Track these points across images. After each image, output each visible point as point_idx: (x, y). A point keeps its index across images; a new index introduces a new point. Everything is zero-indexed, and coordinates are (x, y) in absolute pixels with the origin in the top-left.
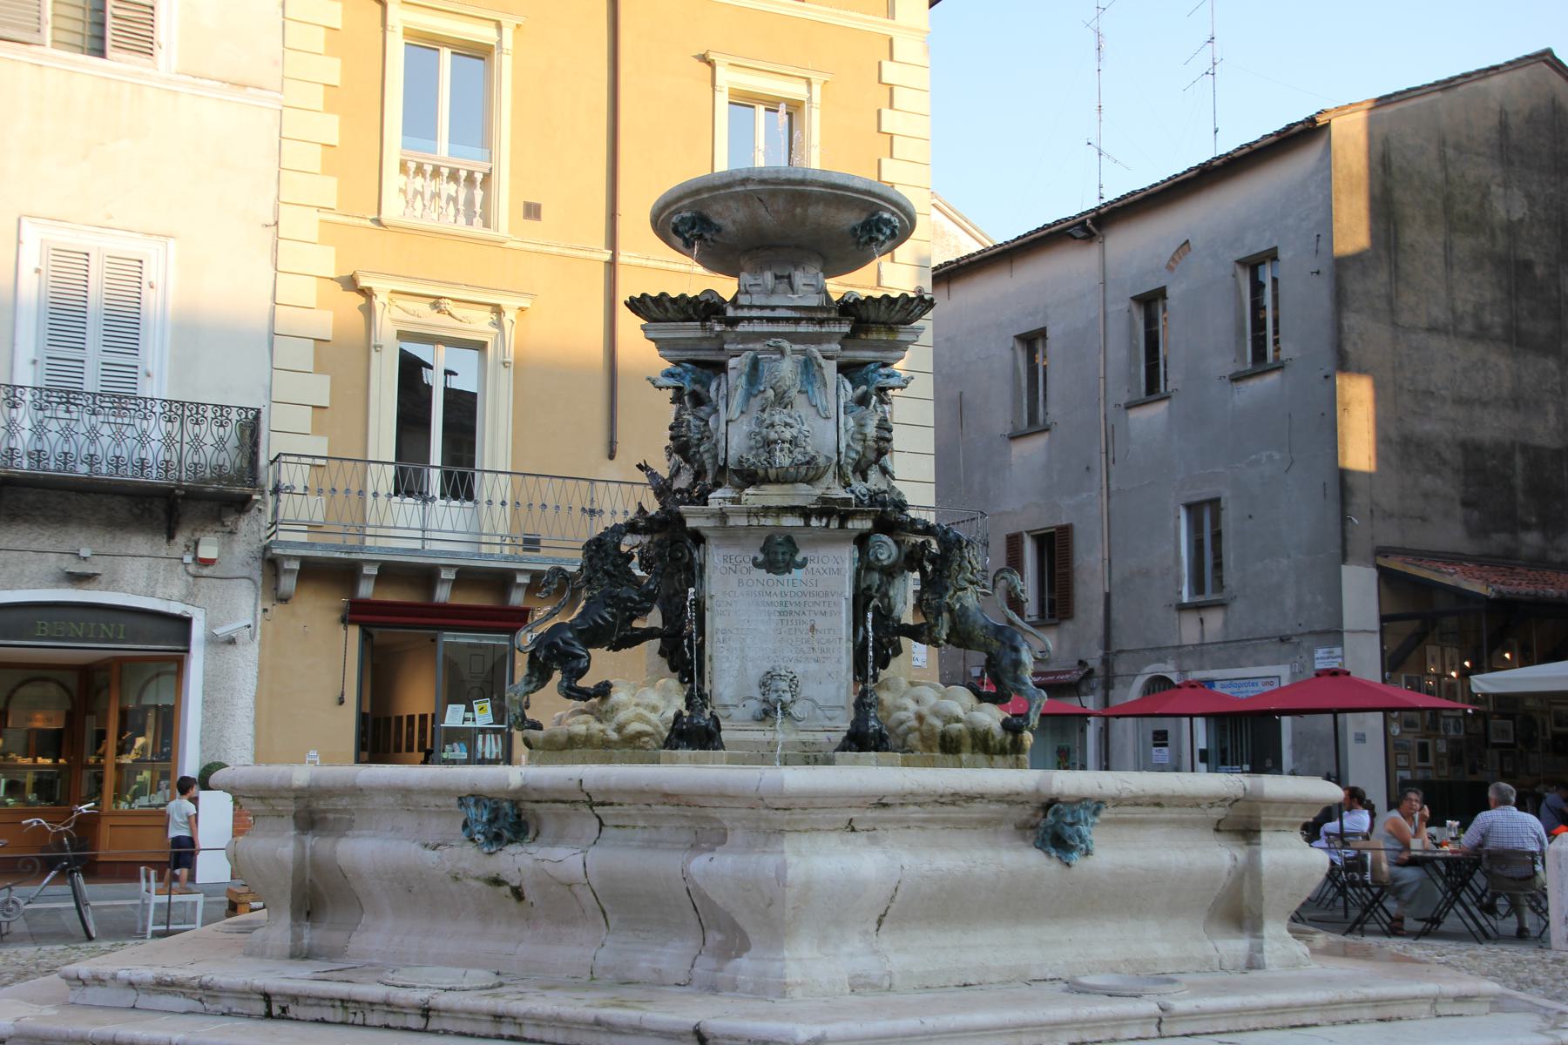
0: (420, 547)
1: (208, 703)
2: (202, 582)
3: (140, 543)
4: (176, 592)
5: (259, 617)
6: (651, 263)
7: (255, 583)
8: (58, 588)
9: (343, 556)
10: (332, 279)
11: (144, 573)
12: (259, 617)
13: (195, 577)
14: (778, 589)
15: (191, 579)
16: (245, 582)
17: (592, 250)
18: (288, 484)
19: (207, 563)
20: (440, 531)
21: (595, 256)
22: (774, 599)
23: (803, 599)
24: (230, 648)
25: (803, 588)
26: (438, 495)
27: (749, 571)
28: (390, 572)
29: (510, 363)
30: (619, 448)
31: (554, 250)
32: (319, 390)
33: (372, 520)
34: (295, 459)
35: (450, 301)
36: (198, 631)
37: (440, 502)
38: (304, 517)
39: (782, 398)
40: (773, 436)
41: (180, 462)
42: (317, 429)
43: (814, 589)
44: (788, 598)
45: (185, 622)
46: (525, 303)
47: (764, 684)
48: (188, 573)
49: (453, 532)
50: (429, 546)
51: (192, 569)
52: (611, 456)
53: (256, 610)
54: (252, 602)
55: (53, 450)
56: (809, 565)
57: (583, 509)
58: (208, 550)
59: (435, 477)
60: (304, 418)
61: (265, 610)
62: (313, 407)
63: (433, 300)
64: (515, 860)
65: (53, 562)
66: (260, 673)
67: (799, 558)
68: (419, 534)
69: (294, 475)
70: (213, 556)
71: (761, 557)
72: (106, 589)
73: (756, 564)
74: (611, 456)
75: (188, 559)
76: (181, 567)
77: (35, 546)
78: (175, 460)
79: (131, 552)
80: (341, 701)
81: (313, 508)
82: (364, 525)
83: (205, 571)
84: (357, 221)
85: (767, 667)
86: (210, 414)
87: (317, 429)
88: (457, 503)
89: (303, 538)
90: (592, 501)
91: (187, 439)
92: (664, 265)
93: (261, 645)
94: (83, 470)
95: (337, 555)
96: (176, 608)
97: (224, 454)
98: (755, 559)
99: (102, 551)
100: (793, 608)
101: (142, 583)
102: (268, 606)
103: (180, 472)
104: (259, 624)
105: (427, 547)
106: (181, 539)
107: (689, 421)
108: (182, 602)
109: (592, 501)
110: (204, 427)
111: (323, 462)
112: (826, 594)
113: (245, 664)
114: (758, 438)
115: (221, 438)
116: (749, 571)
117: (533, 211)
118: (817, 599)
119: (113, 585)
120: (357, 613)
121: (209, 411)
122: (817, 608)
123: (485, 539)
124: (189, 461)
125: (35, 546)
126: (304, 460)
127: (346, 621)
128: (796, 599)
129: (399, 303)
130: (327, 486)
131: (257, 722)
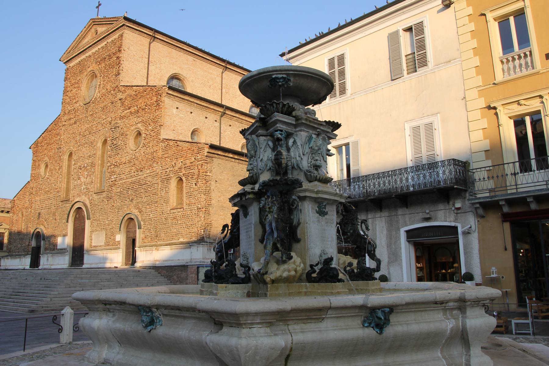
0: (494, 195)
1: (465, 253)
2: (459, 215)
3: (441, 206)
5: (476, 224)
7: (473, 212)
8: (423, 222)
9: (490, 200)
10: (484, 108)
11: (443, 215)
13: (457, 213)
15: (455, 215)
16: (471, 213)
19: (458, 209)
24: (469, 235)
26: (536, 169)
28: (511, 202)
33: (508, 184)
34: (479, 170)
35: (523, 101)
36: (460, 230)
37: (536, 172)
38: (485, 188)
41: (434, 181)
42: (487, 158)
45: (456, 228)
48: (455, 213)
49: (533, 183)
51: (455, 211)
53: (475, 221)
54: (473, 219)
58: (458, 205)
59: (533, 163)
61: (478, 221)
62: (485, 151)
63: (517, 102)
65: (421, 216)
66: (479, 241)
72: (435, 221)
75: (453, 209)
76: (452, 212)
77: (417, 212)
78: (433, 180)
79: (439, 209)
80: (506, 249)
81: (490, 184)
82: (506, 186)
83: (459, 211)
84: (488, 86)
87: (487, 158)
88: (527, 173)
89: (488, 195)
93: (478, 233)
94: (412, 189)
95: (488, 200)
96: (453, 224)
97: (445, 176)
99: (432, 210)
101: (443, 218)
102: (479, 219)
104: (477, 226)
105: (518, 191)
106: (451, 203)
108: (454, 222)
110: (445, 167)
111: (491, 168)
113: (474, 238)
115: (444, 171)
119: (436, 220)
120: (506, 218)
121: (440, 163)
125: (417, 212)
126: (482, 169)
127: (504, 221)
129: (507, 107)
130: (495, 176)
131: (480, 258)
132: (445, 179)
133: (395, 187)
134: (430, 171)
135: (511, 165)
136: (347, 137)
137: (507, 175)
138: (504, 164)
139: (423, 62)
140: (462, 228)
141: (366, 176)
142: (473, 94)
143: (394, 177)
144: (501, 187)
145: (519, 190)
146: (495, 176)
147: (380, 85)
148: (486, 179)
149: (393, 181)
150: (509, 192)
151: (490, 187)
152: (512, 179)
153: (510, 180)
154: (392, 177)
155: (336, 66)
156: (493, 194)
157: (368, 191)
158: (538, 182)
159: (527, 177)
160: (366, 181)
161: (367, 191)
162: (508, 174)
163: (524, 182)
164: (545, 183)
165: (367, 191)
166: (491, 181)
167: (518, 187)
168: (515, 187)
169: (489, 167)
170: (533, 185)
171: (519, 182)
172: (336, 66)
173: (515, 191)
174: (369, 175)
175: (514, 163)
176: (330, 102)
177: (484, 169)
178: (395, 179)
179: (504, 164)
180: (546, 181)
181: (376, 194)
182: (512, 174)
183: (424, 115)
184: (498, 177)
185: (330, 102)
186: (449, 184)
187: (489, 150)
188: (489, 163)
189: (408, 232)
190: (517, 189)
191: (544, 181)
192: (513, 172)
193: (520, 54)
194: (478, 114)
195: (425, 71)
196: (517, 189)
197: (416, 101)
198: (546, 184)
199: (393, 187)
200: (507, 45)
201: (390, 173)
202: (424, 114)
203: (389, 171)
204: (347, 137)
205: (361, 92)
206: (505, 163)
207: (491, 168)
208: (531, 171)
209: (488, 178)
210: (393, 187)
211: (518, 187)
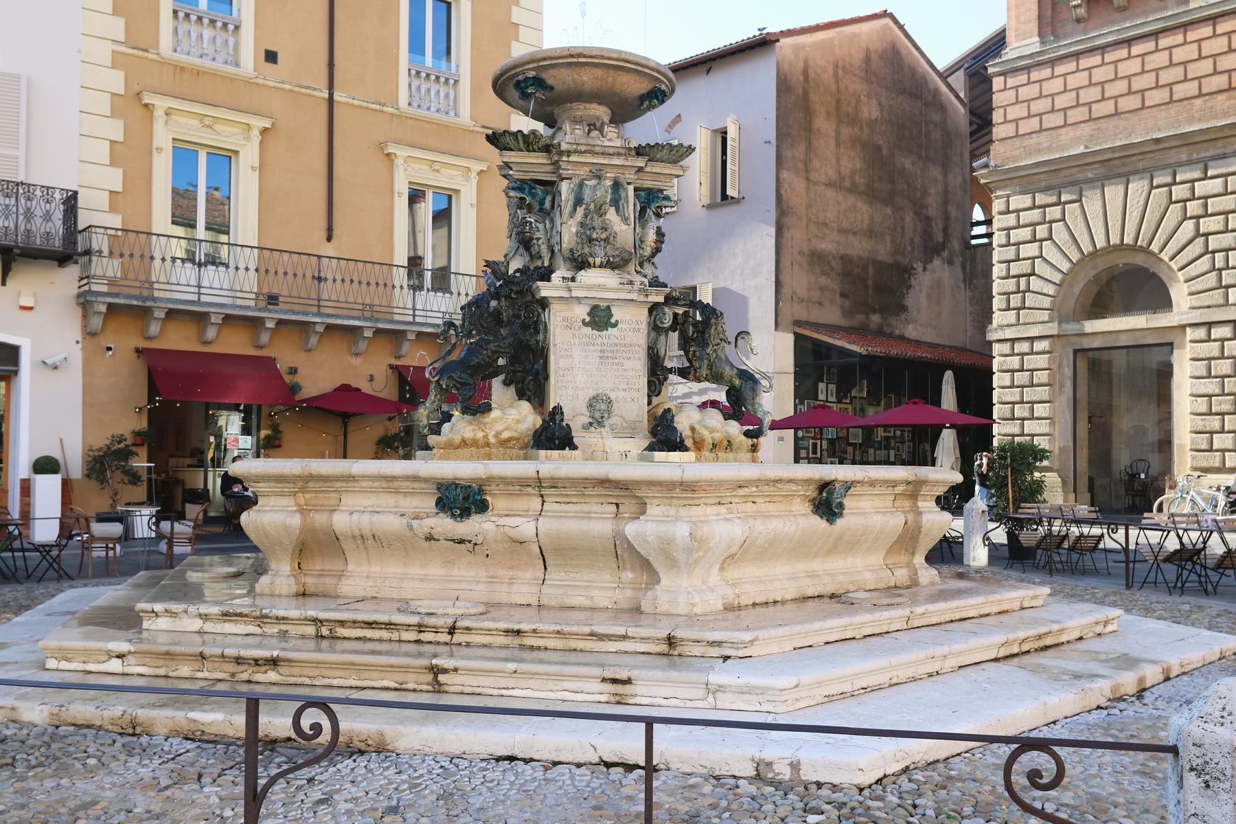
6: (355, 102)
9: (140, 304)
14: (599, 341)
17: (315, 89)
18: (97, 249)
20: (241, 291)
21: (316, 93)
22: (596, 348)
23: (616, 348)
25: (616, 341)
27: (580, 328)
30: (336, 232)
31: (288, 87)
32: (114, 179)
39: (600, 209)
40: (594, 236)
42: (113, 208)
43: (623, 342)
44: (606, 348)
46: (267, 124)
47: (591, 405)
50: (203, 298)
52: (329, 239)
56: (620, 326)
57: (313, 277)
62: (110, 191)
64: (474, 526)
67: (613, 321)
68: (196, 290)
69: (100, 242)
71: (588, 319)
73: (585, 324)
74: (329, 239)
78: (12, 226)
85: (592, 393)
86: (38, 193)
87: (113, 208)
90: (319, 271)
91: (21, 211)
92: (365, 104)
97: (50, 224)
98: (584, 320)
100: (609, 354)
103: (17, 236)
107: (531, 222)
109: (319, 271)
110: (34, 202)
111: (120, 233)
112: (630, 345)
114: (583, 237)
115: (48, 212)
116: (580, 328)
117: (271, 57)
118: (625, 349)
122: (625, 355)
128: (611, 348)
132: (48, 233)
134: (7, 202)
148: (106, 253)
151: (110, 273)
156: (115, 290)
166: (116, 262)
169: (117, 229)
170: (230, 294)
177: (102, 231)
178: (29, 209)
184: (131, 255)
193: (216, 21)
200: (416, 46)
209: (111, 253)
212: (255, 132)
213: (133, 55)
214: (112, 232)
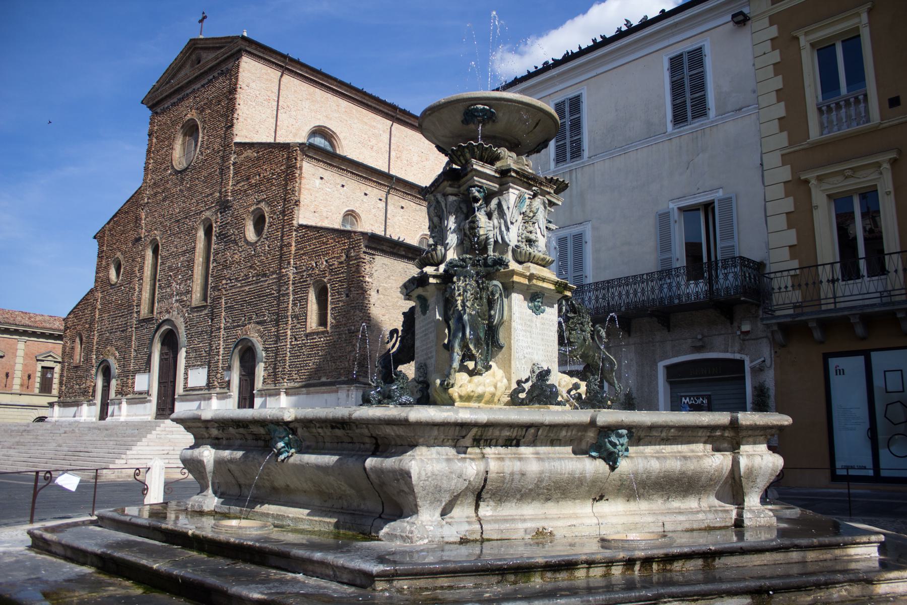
0: (801, 312)
2: (746, 342)
4: (736, 349)
5: (773, 356)
12: (773, 356)
13: (744, 340)
19: (747, 333)
26: (865, 274)
29: (890, 192)
32: (791, 237)
33: (822, 296)
37: (866, 279)
38: (787, 301)
45: (742, 362)
46: (893, 155)
49: (860, 294)
51: (741, 337)
53: (771, 352)
54: (769, 349)
55: (683, 293)
58: (746, 327)
59: (862, 264)
60: (786, 253)
61: (776, 352)
62: (790, 246)
70: (748, 329)
75: (739, 333)
76: (737, 337)
81: (796, 296)
82: (820, 299)
87: (793, 257)
88: (852, 282)
89: (791, 312)
94: (676, 301)
96: (738, 356)
97: (728, 282)
104: (773, 359)
106: (735, 324)
108: (739, 353)
117: (894, 102)
119: (711, 350)
123: (823, 302)
124: (651, 298)
126: (785, 274)
130: (803, 283)
132: (727, 288)
133: (651, 298)
135: (828, 267)
136: (581, 223)
137: (821, 282)
138: (817, 266)
139: (700, 109)
140: (752, 361)
141: (608, 282)
142: (774, 159)
143: (650, 283)
144: (812, 301)
145: (838, 305)
146: (803, 283)
147: (633, 144)
148: (790, 288)
149: (649, 289)
150: (824, 308)
151: (794, 300)
152: (829, 290)
153: (826, 290)
154: (647, 284)
155: (567, 114)
156: (799, 311)
157: (611, 304)
158: (868, 293)
159: (851, 286)
160: (608, 289)
161: (608, 304)
162: (823, 280)
163: (847, 293)
164: (878, 295)
165: (608, 304)
167: (837, 300)
168: (832, 300)
169: (795, 269)
170: (860, 297)
171: (839, 294)
172: (567, 114)
173: (832, 306)
174: (613, 280)
175: (832, 264)
176: (556, 169)
179: (817, 266)
180: (880, 292)
181: (623, 309)
182: (828, 281)
183: (699, 191)
184: (807, 284)
185: (556, 169)
186: (734, 295)
187: (795, 245)
188: (795, 264)
189: (669, 368)
190: (835, 303)
191: (877, 292)
192: (831, 278)
194: (780, 190)
195: (702, 124)
196: (835, 303)
197: (687, 168)
198: (881, 297)
199: (648, 298)
201: (645, 277)
202: (698, 189)
203: (643, 275)
204: (581, 223)
205: (605, 153)
206: (819, 263)
207: (798, 272)
208: (859, 278)
209: (793, 286)
210: (648, 298)
211: (837, 300)
212: (886, 166)
213: (795, 152)
214: (792, 273)
